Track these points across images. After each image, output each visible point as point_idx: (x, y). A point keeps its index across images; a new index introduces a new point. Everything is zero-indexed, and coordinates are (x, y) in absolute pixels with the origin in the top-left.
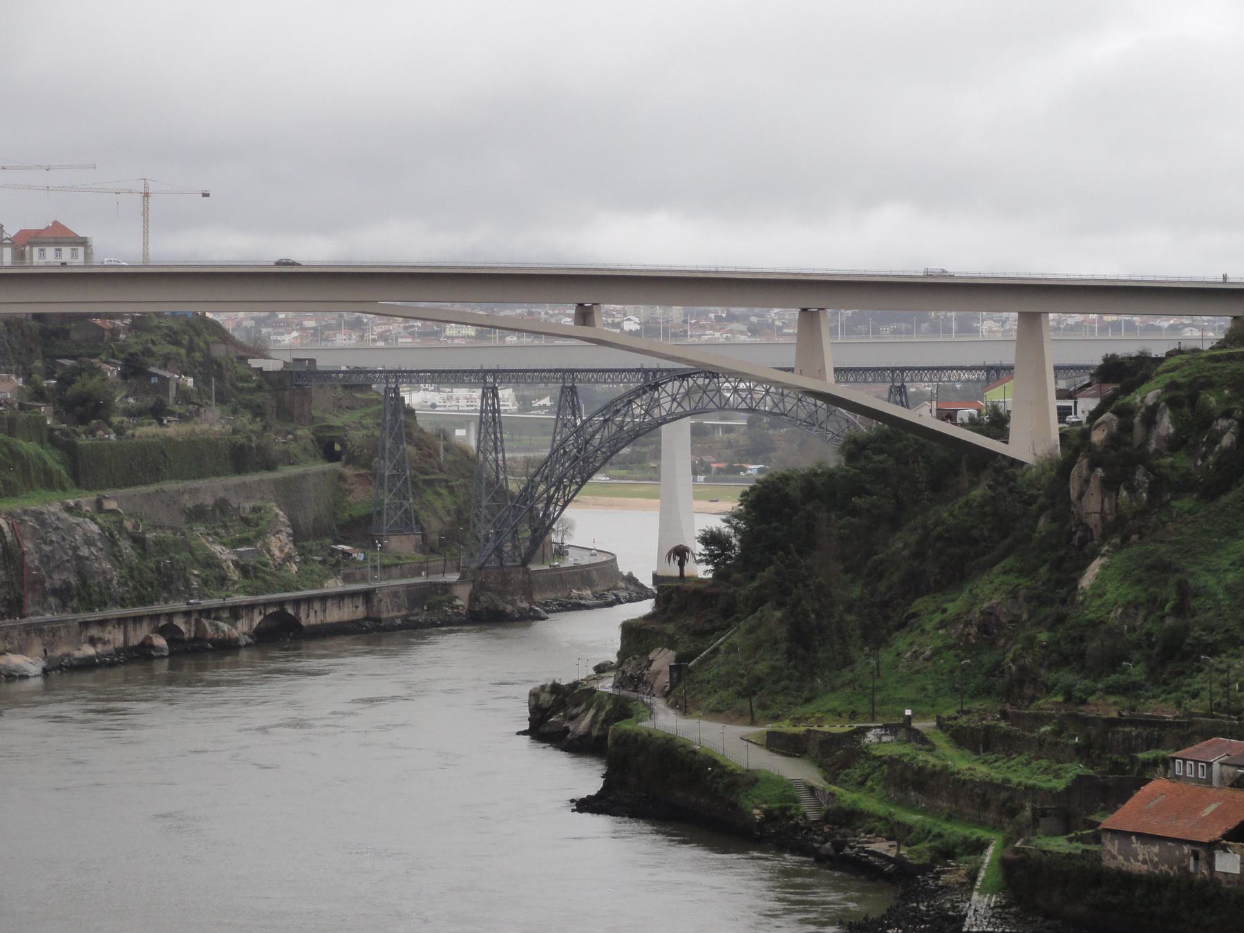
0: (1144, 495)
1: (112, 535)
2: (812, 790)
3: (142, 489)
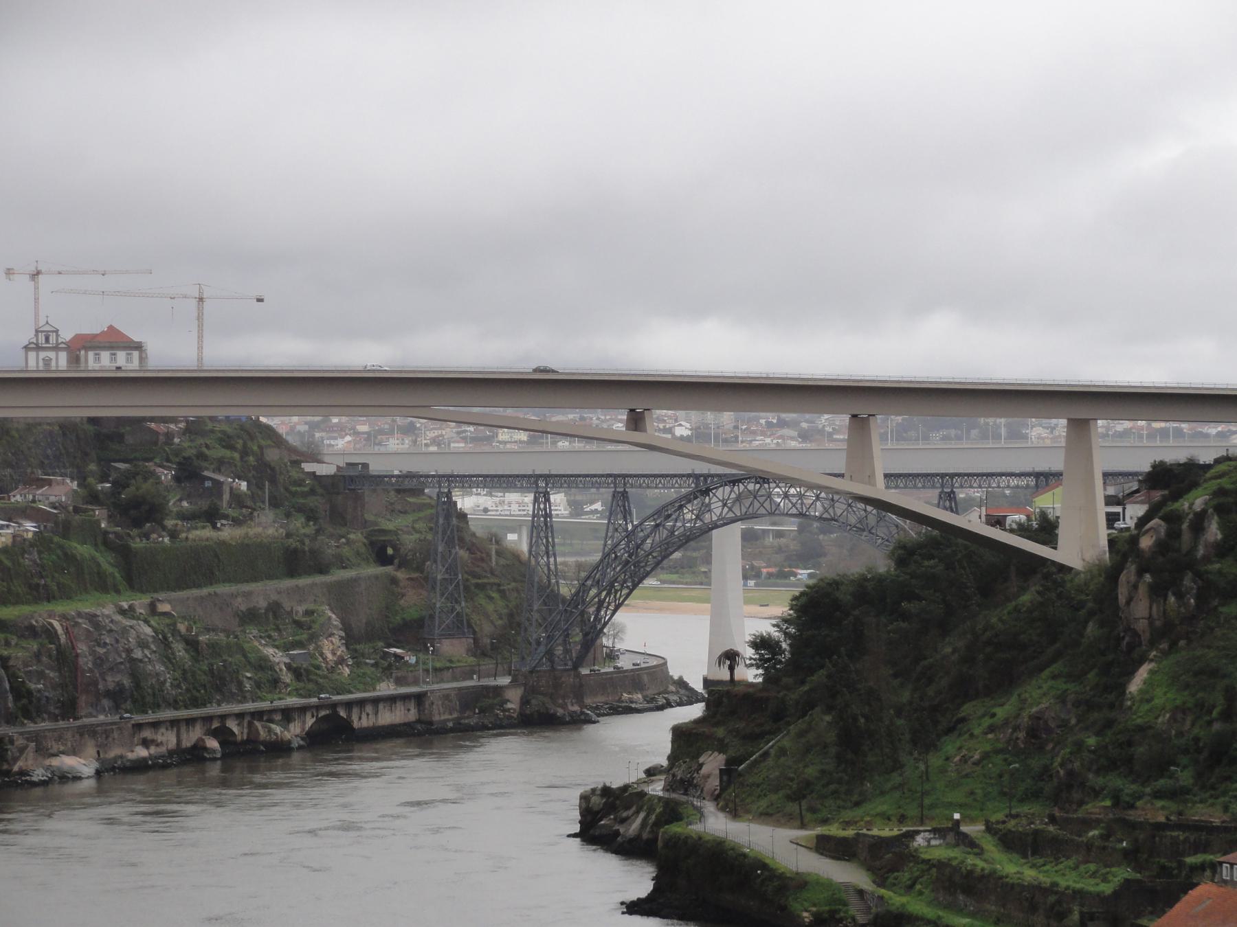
0: (1192, 601)
1: (165, 638)
2: (861, 893)
3: (195, 592)
